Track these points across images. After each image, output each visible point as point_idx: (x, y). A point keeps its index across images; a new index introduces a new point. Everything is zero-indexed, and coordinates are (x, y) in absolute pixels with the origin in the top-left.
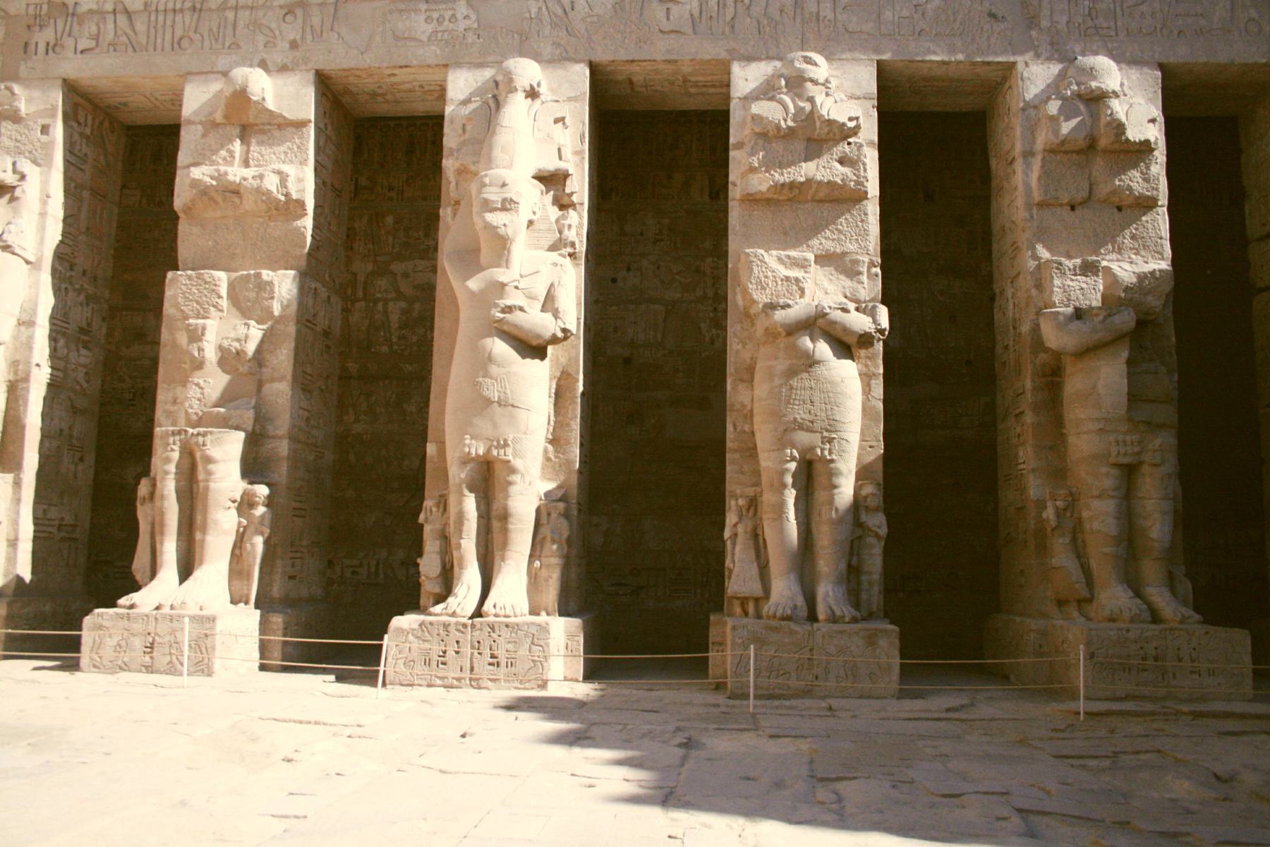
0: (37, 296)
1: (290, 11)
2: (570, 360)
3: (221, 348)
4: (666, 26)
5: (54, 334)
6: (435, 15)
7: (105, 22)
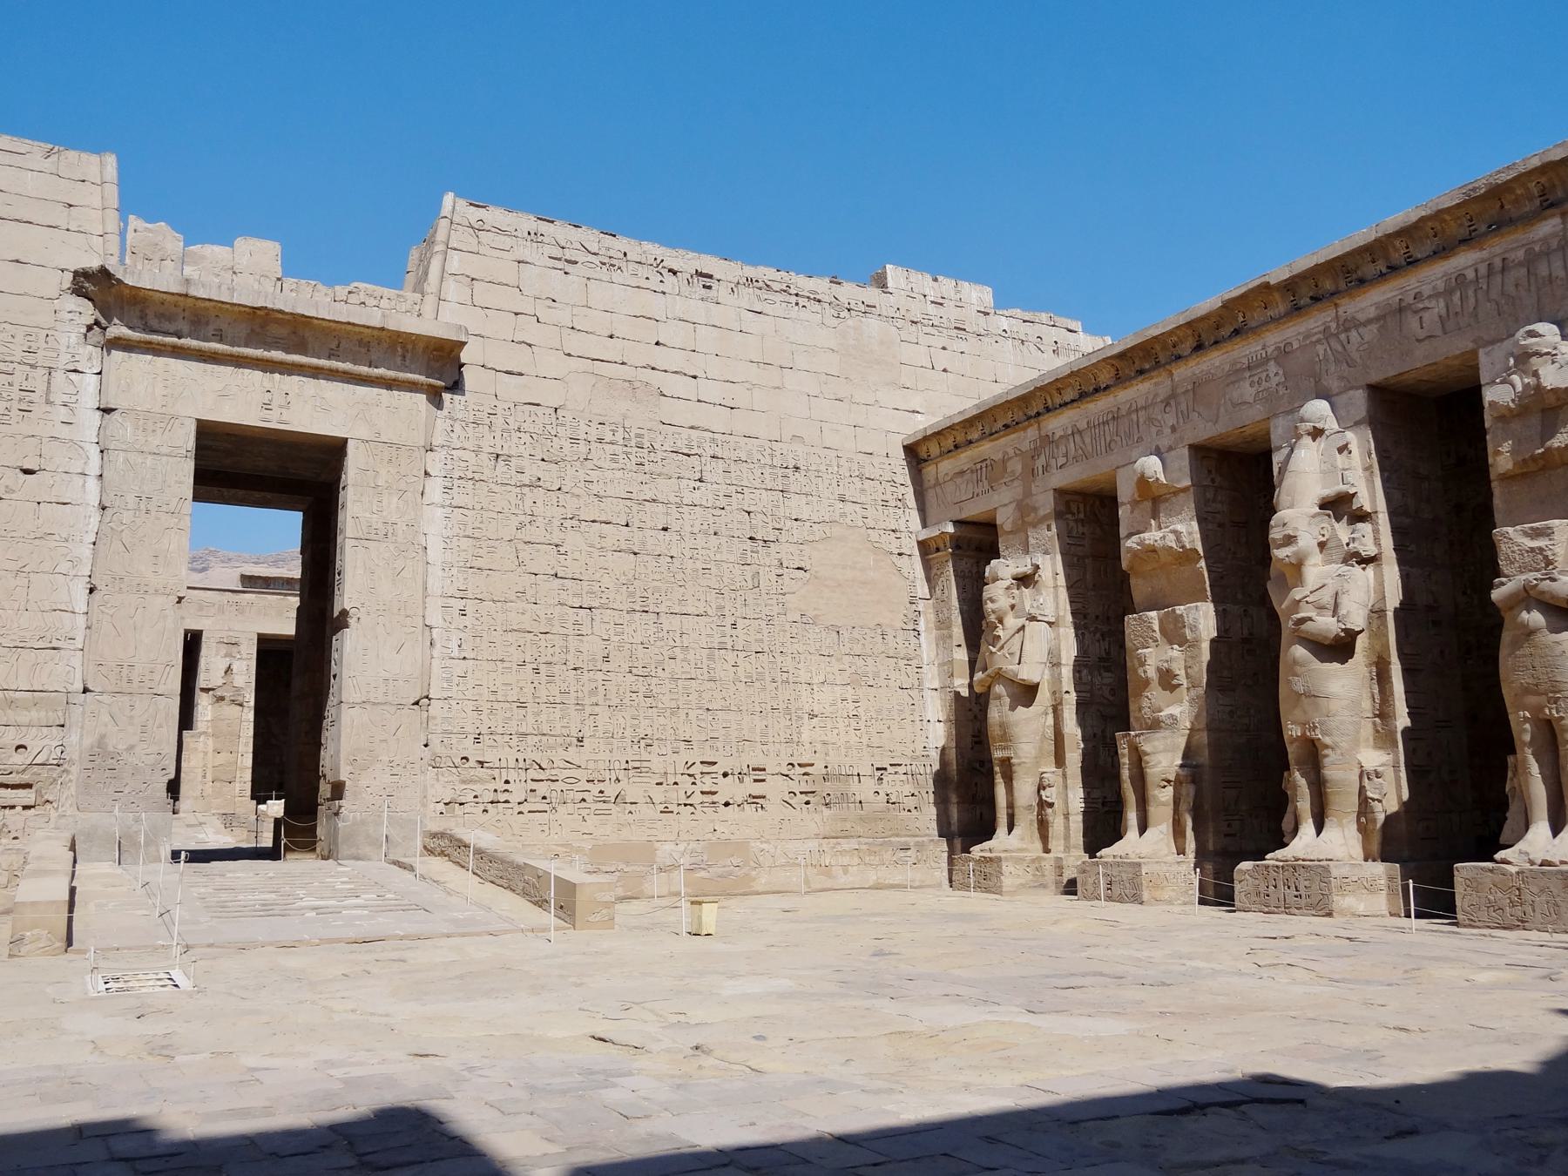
0: (1059, 645)
1: (1168, 404)
2: (1382, 645)
3: (1159, 670)
4: (1422, 334)
5: (1078, 668)
6: (1256, 378)
7: (1069, 443)
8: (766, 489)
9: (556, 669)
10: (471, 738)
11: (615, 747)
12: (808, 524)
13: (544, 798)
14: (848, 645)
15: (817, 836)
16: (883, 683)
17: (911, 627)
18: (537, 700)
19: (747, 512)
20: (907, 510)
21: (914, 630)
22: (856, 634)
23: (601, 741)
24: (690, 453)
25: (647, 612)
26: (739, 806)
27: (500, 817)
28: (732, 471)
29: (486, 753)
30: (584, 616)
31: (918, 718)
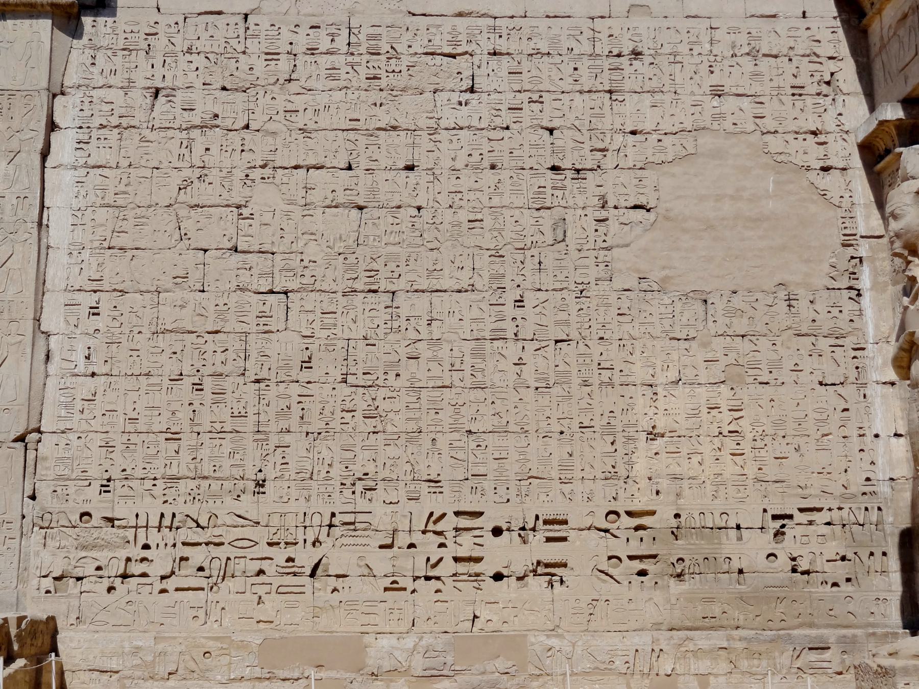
8: (581, 92)
9: (228, 384)
10: (96, 486)
11: (314, 493)
12: (655, 136)
13: (201, 569)
14: (721, 320)
15: (657, 626)
16: (789, 377)
17: (845, 283)
18: (196, 429)
19: (547, 129)
20: (840, 99)
21: (850, 288)
22: (737, 301)
23: (292, 484)
24: (454, 52)
25: (375, 291)
26: (520, 579)
27: (133, 597)
28: (525, 71)
29: (116, 507)
30: (275, 304)
31: (855, 433)
